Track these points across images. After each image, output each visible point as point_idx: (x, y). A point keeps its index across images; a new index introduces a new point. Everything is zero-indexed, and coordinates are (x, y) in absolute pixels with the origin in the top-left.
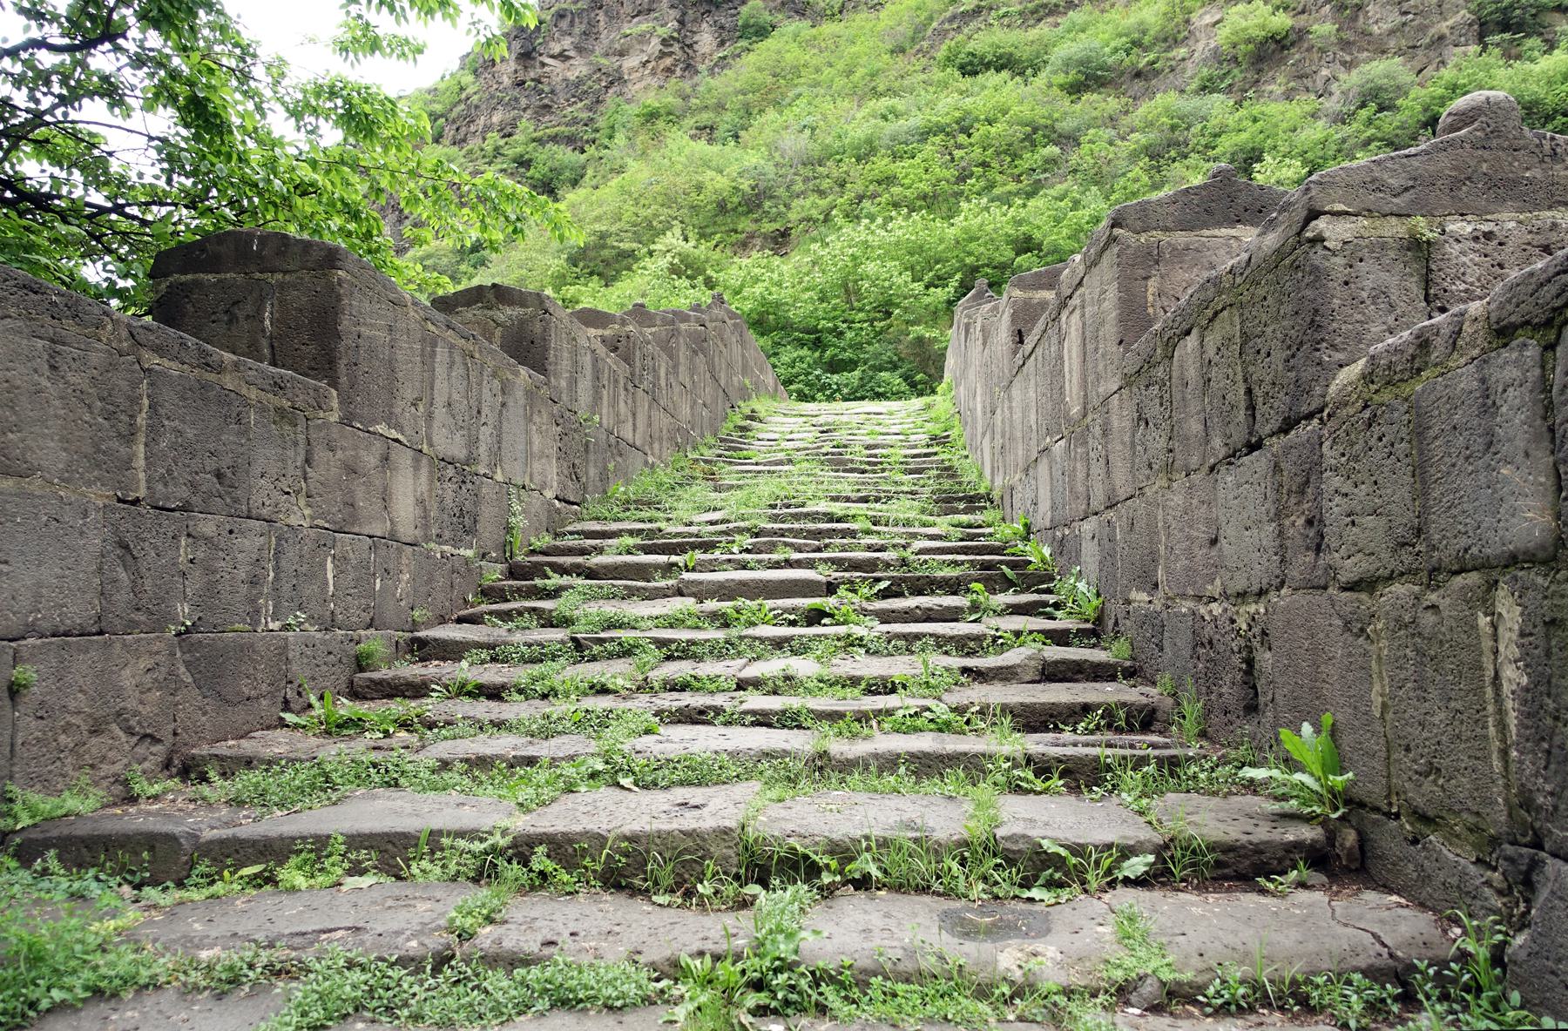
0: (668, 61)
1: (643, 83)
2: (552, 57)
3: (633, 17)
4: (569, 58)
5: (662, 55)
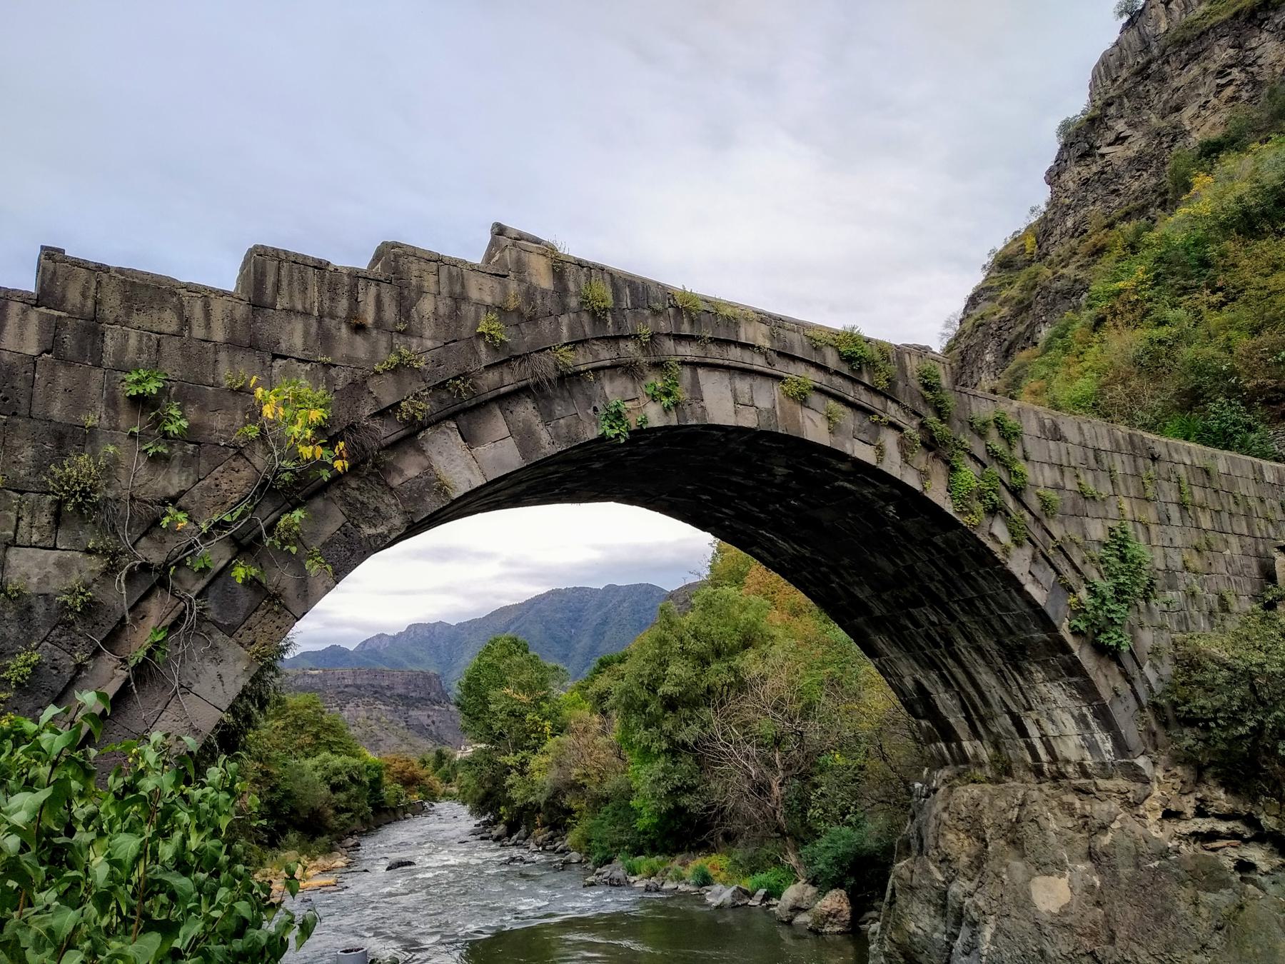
0: (1229, 91)
1: (1208, 124)
2: (1110, 145)
3: (1182, 69)
4: (1126, 138)
5: (1221, 88)
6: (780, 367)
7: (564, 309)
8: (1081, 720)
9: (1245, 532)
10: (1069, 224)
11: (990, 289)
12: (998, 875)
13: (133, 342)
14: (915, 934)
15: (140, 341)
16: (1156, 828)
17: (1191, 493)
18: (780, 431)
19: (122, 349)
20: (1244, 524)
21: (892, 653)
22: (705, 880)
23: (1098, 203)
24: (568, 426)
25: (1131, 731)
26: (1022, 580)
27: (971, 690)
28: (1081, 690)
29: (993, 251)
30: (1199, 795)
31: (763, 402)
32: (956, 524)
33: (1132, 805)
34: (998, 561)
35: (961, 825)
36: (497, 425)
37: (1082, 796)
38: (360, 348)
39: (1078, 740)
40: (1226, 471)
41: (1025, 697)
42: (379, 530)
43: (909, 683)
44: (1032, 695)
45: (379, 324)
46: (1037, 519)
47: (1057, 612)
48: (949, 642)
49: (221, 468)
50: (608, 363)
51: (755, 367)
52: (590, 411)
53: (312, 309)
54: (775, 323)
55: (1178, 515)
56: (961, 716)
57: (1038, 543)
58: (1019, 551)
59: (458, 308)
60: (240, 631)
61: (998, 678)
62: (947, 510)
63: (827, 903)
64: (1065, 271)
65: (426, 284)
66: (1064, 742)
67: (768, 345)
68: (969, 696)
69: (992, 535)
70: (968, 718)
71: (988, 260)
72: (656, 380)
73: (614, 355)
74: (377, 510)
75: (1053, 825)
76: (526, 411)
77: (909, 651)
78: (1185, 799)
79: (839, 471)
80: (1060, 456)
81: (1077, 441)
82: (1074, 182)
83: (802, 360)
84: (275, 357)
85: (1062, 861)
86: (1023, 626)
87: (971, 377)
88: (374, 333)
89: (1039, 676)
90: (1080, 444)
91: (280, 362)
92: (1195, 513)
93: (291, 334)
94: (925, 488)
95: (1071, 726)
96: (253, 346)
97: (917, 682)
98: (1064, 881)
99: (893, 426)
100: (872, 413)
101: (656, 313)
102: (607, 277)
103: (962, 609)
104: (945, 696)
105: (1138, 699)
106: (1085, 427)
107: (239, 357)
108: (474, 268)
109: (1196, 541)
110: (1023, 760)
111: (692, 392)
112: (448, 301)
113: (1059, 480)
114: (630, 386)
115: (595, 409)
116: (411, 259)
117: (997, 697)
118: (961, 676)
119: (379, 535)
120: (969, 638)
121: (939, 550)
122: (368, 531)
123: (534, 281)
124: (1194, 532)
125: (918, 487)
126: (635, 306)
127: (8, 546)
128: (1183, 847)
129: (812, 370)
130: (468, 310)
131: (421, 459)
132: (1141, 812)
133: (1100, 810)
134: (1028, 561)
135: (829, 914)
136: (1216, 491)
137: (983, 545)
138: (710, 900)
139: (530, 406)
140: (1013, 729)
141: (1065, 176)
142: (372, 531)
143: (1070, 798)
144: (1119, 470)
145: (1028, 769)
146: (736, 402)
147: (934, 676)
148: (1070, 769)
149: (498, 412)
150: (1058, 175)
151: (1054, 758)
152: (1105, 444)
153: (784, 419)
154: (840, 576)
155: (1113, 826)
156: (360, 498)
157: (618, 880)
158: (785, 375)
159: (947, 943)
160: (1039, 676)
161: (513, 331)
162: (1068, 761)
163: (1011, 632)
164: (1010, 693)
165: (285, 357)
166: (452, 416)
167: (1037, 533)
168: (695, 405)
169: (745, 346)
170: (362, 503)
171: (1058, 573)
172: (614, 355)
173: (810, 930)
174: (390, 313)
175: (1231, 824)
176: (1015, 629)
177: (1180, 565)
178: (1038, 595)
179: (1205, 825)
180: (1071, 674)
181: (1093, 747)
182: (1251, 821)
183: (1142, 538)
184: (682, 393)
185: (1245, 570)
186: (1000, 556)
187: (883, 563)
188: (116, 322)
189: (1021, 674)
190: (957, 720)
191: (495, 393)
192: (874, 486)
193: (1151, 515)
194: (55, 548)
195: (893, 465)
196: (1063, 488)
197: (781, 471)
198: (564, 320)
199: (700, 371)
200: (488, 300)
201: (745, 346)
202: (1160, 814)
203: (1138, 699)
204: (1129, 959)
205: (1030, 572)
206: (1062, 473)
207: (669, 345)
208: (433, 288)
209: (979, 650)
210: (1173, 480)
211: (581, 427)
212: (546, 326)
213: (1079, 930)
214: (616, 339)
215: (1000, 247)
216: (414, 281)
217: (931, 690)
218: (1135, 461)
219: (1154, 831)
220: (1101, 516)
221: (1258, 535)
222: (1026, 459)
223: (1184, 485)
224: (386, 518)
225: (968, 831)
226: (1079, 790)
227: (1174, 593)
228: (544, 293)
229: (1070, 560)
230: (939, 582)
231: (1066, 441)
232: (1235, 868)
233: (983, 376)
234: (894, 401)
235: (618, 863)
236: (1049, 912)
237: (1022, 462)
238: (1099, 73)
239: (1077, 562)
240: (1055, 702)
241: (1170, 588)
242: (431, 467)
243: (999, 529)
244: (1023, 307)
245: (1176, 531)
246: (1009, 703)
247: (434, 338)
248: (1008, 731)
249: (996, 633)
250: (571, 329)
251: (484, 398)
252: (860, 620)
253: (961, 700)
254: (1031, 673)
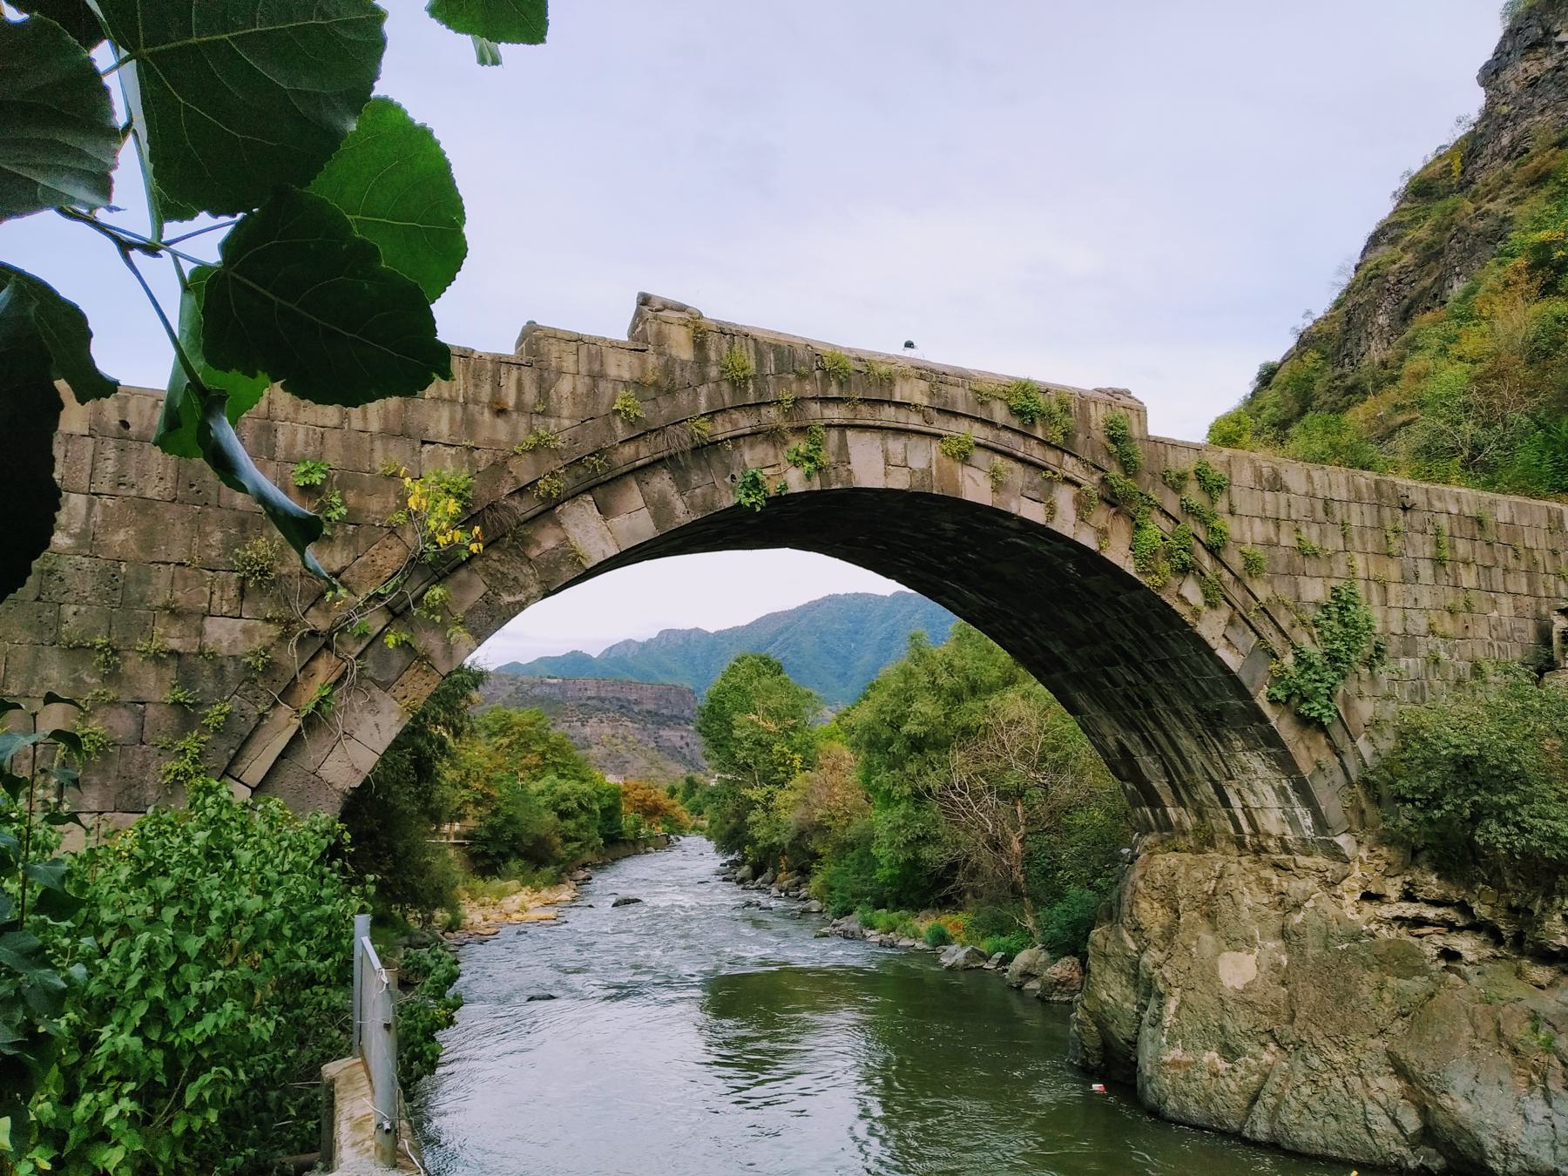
6: (940, 425)
7: (704, 380)
8: (1281, 793)
9: (1525, 590)
10: (1505, 141)
11: (1399, 224)
12: (1187, 948)
13: (301, 436)
14: (1106, 1003)
15: (307, 435)
16: (1353, 909)
17: (1453, 548)
18: (935, 492)
19: (292, 445)
20: (1524, 581)
21: (1093, 711)
22: (941, 939)
23: (1549, 112)
24: (704, 495)
25: (1332, 805)
26: (1213, 644)
27: (1172, 754)
28: (1280, 762)
30: (1408, 879)
31: (918, 462)
32: (1139, 586)
33: (1330, 885)
34: (1185, 624)
35: (1155, 894)
36: (633, 496)
37: (1280, 872)
38: (502, 430)
39: (1279, 813)
40: (1508, 520)
41: (1226, 766)
42: (518, 598)
43: (1111, 741)
44: (1232, 763)
45: (520, 406)
46: (1238, 579)
47: (1253, 680)
48: (1148, 704)
49: (376, 546)
50: (748, 431)
51: (910, 427)
52: (728, 480)
53: (458, 396)
54: (935, 377)
55: (1430, 572)
56: (1164, 781)
57: (1237, 605)
58: (1214, 613)
59: (595, 386)
60: (394, 687)
61: (1198, 744)
62: (1127, 571)
63: (1057, 970)
64: (1491, 206)
65: (565, 364)
66: (1265, 814)
67: (925, 403)
68: (1170, 759)
69: (1180, 596)
70: (1171, 783)
72: (800, 445)
73: (755, 423)
74: (515, 579)
75: (1248, 900)
76: (662, 482)
77: (1109, 710)
78: (1390, 881)
79: (1008, 527)
80: (1278, 508)
81: (1302, 491)
82: (1517, 83)
83: (965, 416)
84: (424, 443)
85: (1252, 938)
86: (1218, 690)
87: (1358, 345)
88: (515, 415)
89: (1238, 744)
90: (1307, 494)
91: (428, 447)
92: (1454, 570)
93: (439, 421)
94: (1101, 548)
95: (1272, 800)
96: (404, 434)
97: (1117, 740)
98: (1253, 957)
99: (1069, 481)
100: (1045, 469)
101: (801, 377)
102: (751, 343)
103: (1157, 671)
104: (1148, 759)
105: (1347, 774)
106: (1316, 475)
107: (392, 444)
108: (615, 345)
109: (1450, 602)
110: (1225, 831)
111: (839, 455)
112: (587, 380)
113: (1272, 535)
114: (771, 452)
115: (733, 477)
116: (551, 340)
117: (1198, 763)
118: (1162, 740)
119: (518, 602)
120: (1167, 700)
121: (1127, 610)
122: (507, 598)
123: (674, 352)
124: (1450, 591)
125: (1094, 546)
126: (779, 371)
127: (204, 616)
128: (1384, 931)
129: (977, 426)
130: (605, 387)
131: (558, 531)
132: (1339, 892)
133: (1293, 887)
134: (1223, 624)
135: (1058, 982)
136: (1489, 544)
137: (1168, 606)
138: (943, 960)
139: (666, 476)
140: (1215, 798)
141: (1507, 75)
142: (511, 599)
143: (1268, 873)
144: (1355, 521)
145: (1230, 840)
146: (887, 463)
147: (1136, 738)
148: (1271, 843)
149: (634, 485)
150: (1496, 73)
151: (1256, 831)
152: (1342, 493)
153: (940, 479)
154: (1032, 629)
155: (1306, 905)
156: (501, 569)
157: (853, 933)
158: (944, 433)
159: (1137, 1014)
160: (1238, 744)
161: (649, 405)
162: (1269, 835)
163: (1207, 697)
164: (1210, 760)
165: (433, 443)
166: (589, 490)
167: (1237, 594)
168: (841, 468)
169: (899, 405)
170: (502, 573)
171: (1260, 637)
172: (755, 423)
173: (1038, 997)
174: (530, 395)
175: (1441, 911)
176: (1211, 694)
177: (1423, 629)
178: (1232, 660)
179: (1410, 910)
180: (1270, 745)
181: (1294, 822)
182: (1464, 908)
183: (1376, 600)
184: (827, 457)
185: (1516, 635)
186: (1188, 619)
187: (1071, 618)
188: (286, 419)
189: (1221, 742)
190: (1160, 785)
191: (631, 467)
192: (1050, 544)
193: (1393, 571)
194: (240, 617)
195: (1066, 524)
196: (1277, 545)
197: (948, 526)
198: (703, 391)
199: (849, 433)
200: (626, 376)
201: (899, 405)
202: (1358, 895)
203: (1347, 774)
204: (1305, 1039)
205: (1224, 636)
206: (1278, 527)
207: (815, 408)
208: (572, 369)
209: (1178, 713)
210: (1429, 532)
211: (717, 495)
212: (683, 398)
213: (1260, 1008)
214: (758, 405)
215: (1417, 167)
216: (554, 364)
217: (1133, 752)
218: (1379, 511)
219: (1350, 913)
220: (1323, 573)
221: (1543, 594)
222: (1232, 513)
223: (1445, 541)
224: (524, 587)
225: (1162, 900)
226: (1276, 866)
227: (1411, 661)
228: (683, 364)
229: (1276, 623)
230: (1130, 640)
231: (1288, 491)
232: (1439, 956)
233: (1373, 344)
234: (1071, 455)
235: (856, 915)
236: (1233, 988)
237: (1227, 517)
239: (1284, 625)
240: (1255, 772)
241: (1406, 654)
242: (567, 538)
243: (1191, 590)
244: (1431, 254)
245: (1426, 591)
246: (1211, 770)
247: (571, 417)
248: (1211, 800)
249: (1192, 696)
250: (710, 399)
251: (619, 471)
252: (1057, 676)
253: (1164, 764)
254: (1230, 740)
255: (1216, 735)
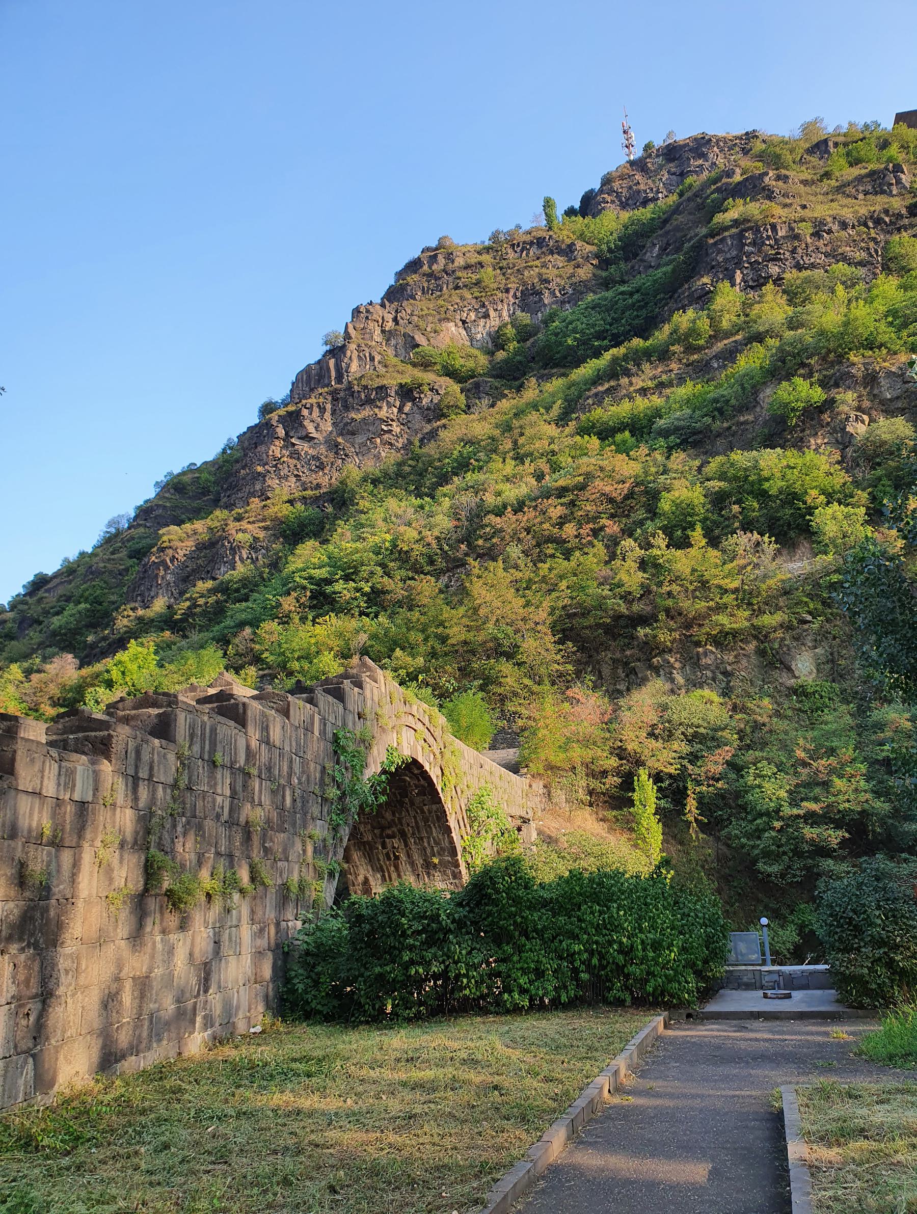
2: (299, 438)
29: (170, 474)
43: (361, 878)
71: (161, 478)
77: (370, 861)
87: (149, 590)
189: (429, 877)
215: (177, 471)
230: (412, 827)
238: (302, 378)
255: (428, 874)
